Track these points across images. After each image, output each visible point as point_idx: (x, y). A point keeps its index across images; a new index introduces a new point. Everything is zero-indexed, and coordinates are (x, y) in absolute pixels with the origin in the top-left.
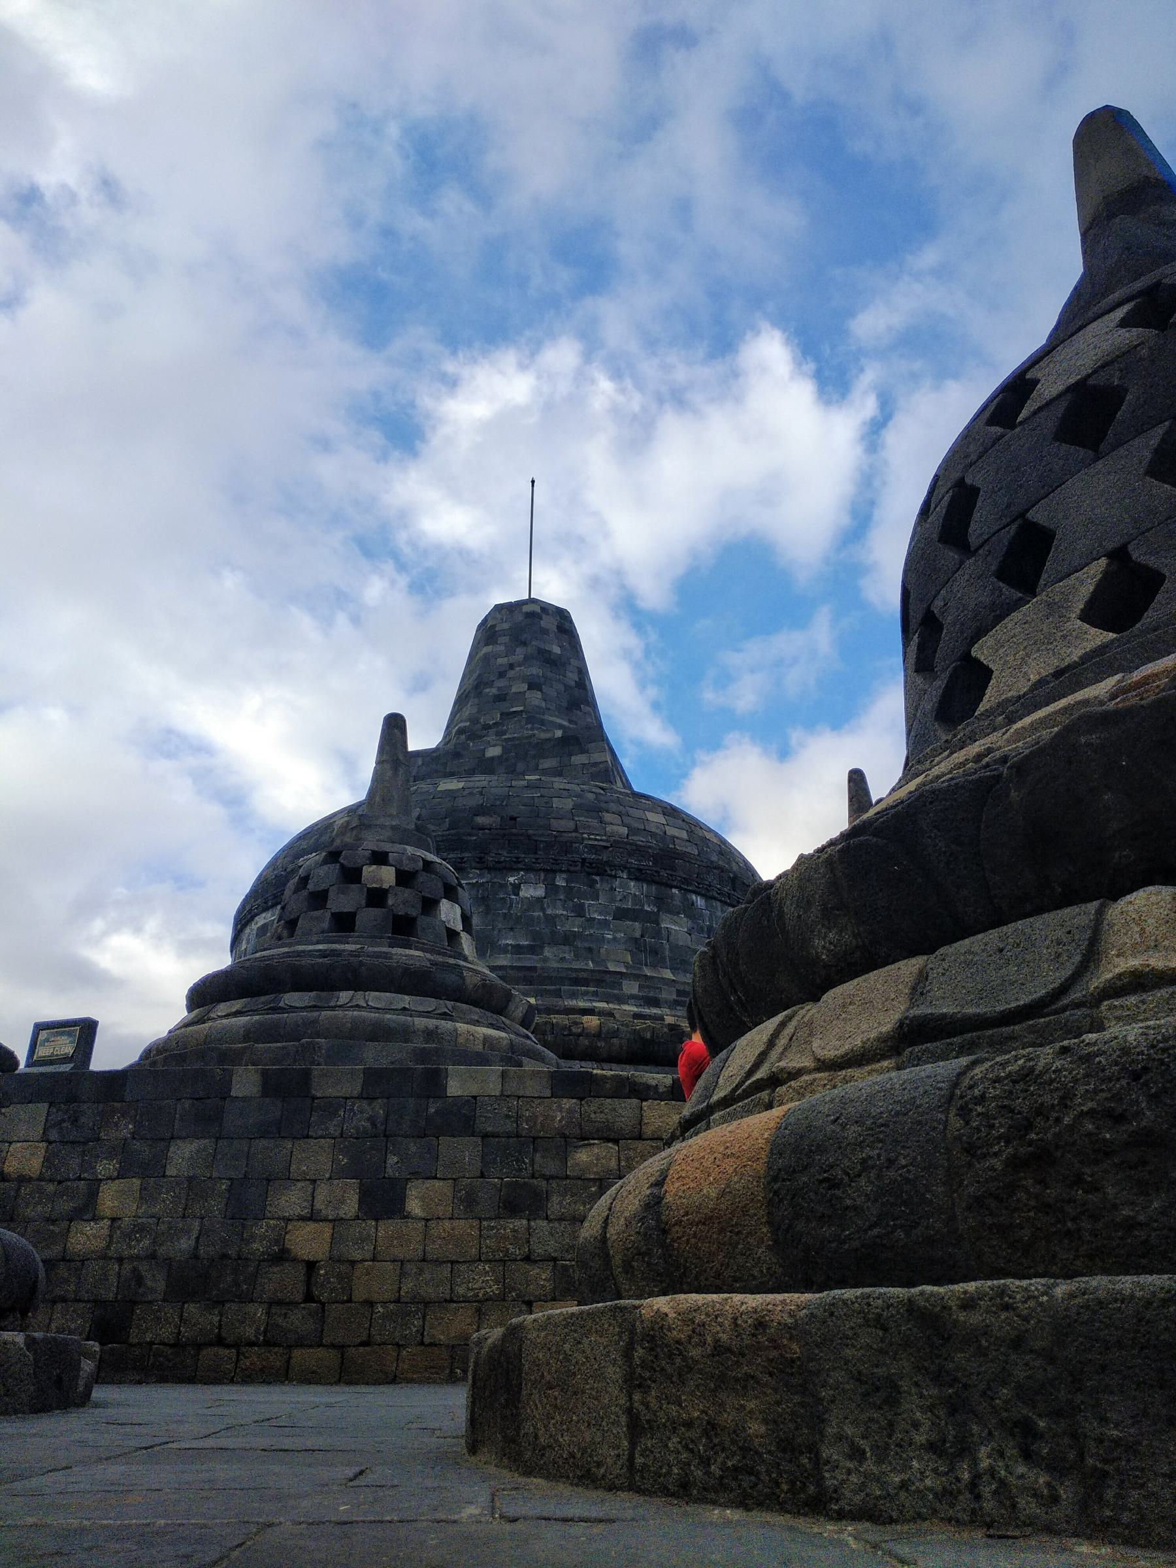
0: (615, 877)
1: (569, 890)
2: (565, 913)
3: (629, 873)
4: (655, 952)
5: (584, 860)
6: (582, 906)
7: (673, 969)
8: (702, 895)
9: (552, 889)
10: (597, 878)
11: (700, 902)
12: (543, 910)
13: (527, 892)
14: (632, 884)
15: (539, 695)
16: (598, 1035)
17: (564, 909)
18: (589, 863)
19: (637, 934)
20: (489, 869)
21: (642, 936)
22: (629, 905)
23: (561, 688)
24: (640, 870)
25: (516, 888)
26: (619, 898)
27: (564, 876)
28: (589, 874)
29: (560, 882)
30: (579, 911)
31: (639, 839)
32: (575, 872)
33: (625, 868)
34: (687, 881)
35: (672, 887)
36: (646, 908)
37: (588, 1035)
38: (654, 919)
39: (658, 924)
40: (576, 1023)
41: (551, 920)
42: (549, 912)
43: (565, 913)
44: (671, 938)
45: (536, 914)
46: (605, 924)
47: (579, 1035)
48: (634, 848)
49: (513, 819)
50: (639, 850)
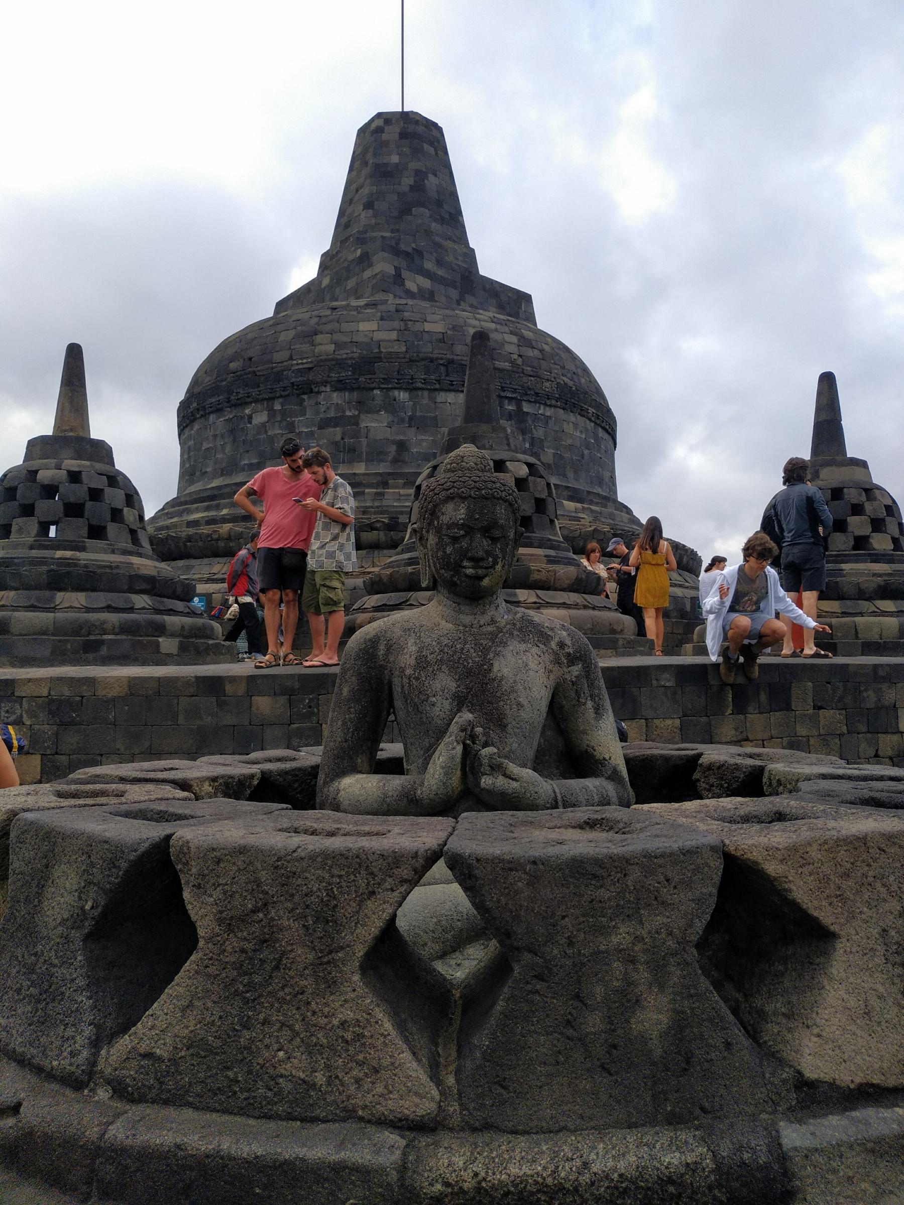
0: (319, 393)
1: (284, 413)
2: (280, 432)
3: (331, 386)
4: (352, 450)
5: (293, 383)
6: (293, 423)
7: (369, 461)
8: (406, 389)
9: (272, 412)
10: (305, 397)
11: (403, 396)
12: (266, 432)
13: (260, 418)
14: (335, 395)
15: (371, 211)
16: (229, 538)
17: (280, 428)
18: (298, 386)
19: (338, 438)
20: (235, 405)
21: (342, 439)
22: (332, 414)
23: (395, 197)
24: (340, 381)
25: (250, 417)
26: (323, 410)
27: (280, 400)
28: (298, 395)
29: (277, 407)
30: (291, 427)
31: (343, 354)
32: (288, 395)
33: (326, 382)
34: (386, 380)
35: (373, 389)
36: (348, 413)
37: (223, 539)
38: (355, 421)
39: (357, 424)
40: (215, 531)
41: (271, 439)
42: (269, 434)
43: (280, 432)
44: (371, 435)
45: (262, 437)
46: (312, 434)
47: (218, 540)
48: (334, 362)
49: (250, 359)
50: (339, 364)
